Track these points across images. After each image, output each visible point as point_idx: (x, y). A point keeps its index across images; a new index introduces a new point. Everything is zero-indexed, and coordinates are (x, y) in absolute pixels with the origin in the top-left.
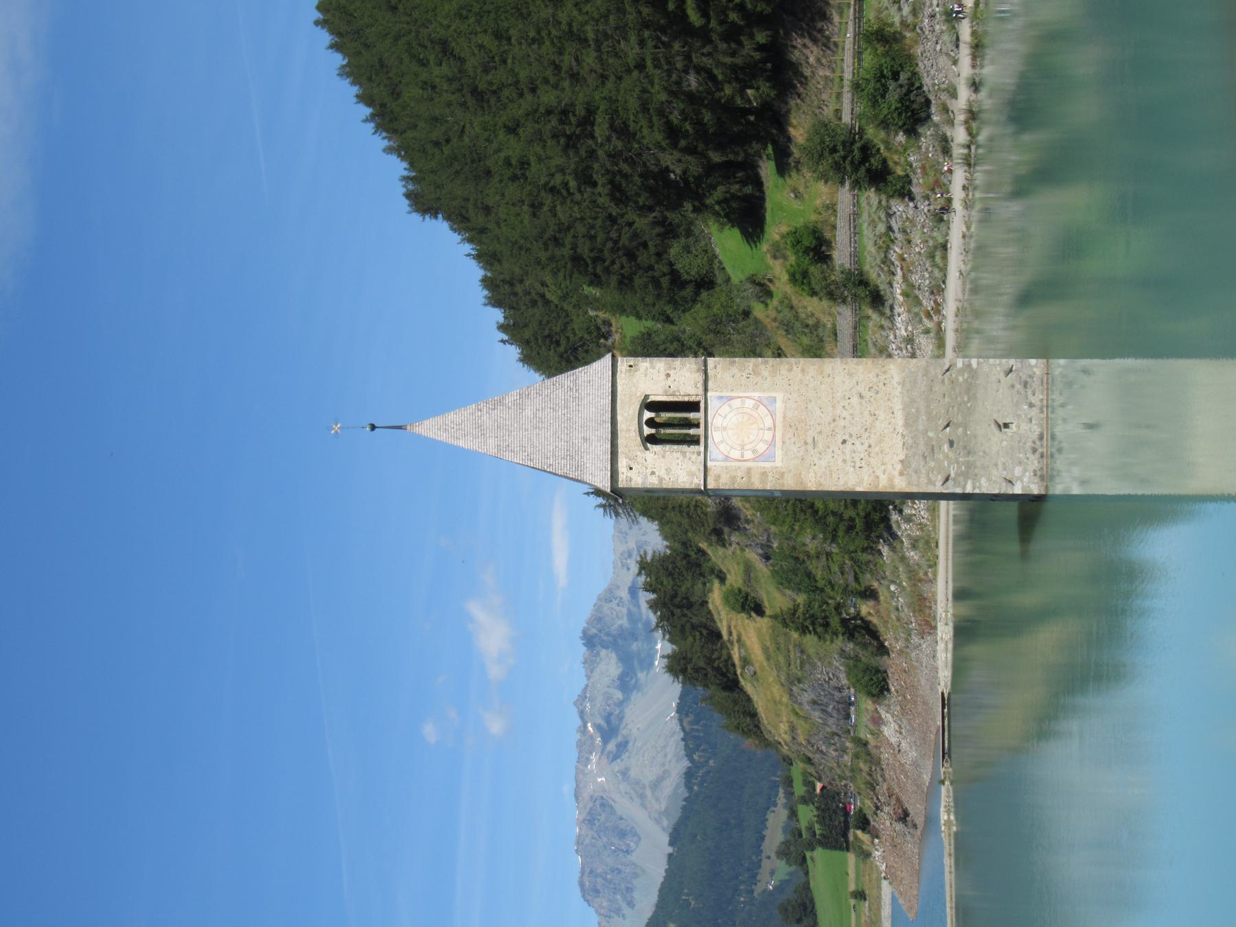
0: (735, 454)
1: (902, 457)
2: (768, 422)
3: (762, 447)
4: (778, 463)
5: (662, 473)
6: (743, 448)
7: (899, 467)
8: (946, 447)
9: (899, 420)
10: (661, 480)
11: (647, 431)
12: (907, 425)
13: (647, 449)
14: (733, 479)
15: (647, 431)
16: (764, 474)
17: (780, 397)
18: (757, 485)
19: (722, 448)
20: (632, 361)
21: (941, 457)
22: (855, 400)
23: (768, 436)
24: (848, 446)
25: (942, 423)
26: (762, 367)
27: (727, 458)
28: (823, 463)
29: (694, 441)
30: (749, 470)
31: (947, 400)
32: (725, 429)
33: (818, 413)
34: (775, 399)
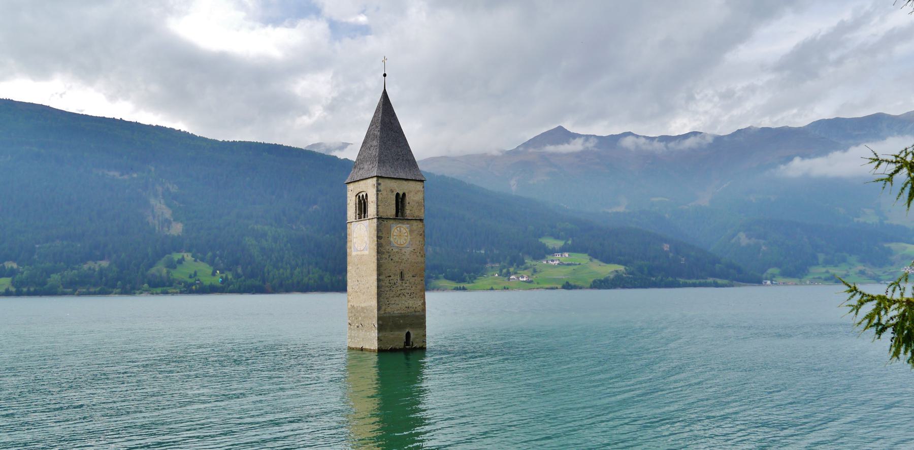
0: (355, 236)
1: (355, 306)
2: (362, 249)
3: (356, 246)
4: (354, 253)
5: (351, 204)
6: (356, 238)
7: (353, 305)
8: (357, 324)
9: (363, 305)
10: (349, 204)
11: (361, 195)
12: (362, 308)
13: (356, 196)
14: (349, 235)
15: (361, 195)
16: (351, 248)
17: (366, 252)
18: (348, 244)
19: (356, 229)
20: (376, 185)
21: (355, 322)
22: (367, 285)
23: (359, 250)
24: (357, 283)
25: (362, 323)
26: (374, 244)
27: (354, 231)
28: (353, 272)
29: (360, 218)
30: (351, 241)
31: (368, 325)
32: (360, 230)
33: (364, 269)
34: (367, 250)
